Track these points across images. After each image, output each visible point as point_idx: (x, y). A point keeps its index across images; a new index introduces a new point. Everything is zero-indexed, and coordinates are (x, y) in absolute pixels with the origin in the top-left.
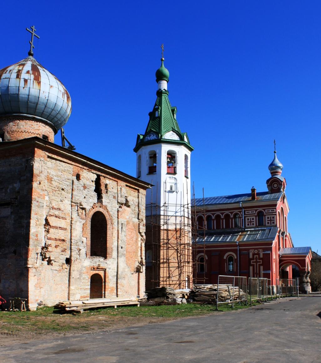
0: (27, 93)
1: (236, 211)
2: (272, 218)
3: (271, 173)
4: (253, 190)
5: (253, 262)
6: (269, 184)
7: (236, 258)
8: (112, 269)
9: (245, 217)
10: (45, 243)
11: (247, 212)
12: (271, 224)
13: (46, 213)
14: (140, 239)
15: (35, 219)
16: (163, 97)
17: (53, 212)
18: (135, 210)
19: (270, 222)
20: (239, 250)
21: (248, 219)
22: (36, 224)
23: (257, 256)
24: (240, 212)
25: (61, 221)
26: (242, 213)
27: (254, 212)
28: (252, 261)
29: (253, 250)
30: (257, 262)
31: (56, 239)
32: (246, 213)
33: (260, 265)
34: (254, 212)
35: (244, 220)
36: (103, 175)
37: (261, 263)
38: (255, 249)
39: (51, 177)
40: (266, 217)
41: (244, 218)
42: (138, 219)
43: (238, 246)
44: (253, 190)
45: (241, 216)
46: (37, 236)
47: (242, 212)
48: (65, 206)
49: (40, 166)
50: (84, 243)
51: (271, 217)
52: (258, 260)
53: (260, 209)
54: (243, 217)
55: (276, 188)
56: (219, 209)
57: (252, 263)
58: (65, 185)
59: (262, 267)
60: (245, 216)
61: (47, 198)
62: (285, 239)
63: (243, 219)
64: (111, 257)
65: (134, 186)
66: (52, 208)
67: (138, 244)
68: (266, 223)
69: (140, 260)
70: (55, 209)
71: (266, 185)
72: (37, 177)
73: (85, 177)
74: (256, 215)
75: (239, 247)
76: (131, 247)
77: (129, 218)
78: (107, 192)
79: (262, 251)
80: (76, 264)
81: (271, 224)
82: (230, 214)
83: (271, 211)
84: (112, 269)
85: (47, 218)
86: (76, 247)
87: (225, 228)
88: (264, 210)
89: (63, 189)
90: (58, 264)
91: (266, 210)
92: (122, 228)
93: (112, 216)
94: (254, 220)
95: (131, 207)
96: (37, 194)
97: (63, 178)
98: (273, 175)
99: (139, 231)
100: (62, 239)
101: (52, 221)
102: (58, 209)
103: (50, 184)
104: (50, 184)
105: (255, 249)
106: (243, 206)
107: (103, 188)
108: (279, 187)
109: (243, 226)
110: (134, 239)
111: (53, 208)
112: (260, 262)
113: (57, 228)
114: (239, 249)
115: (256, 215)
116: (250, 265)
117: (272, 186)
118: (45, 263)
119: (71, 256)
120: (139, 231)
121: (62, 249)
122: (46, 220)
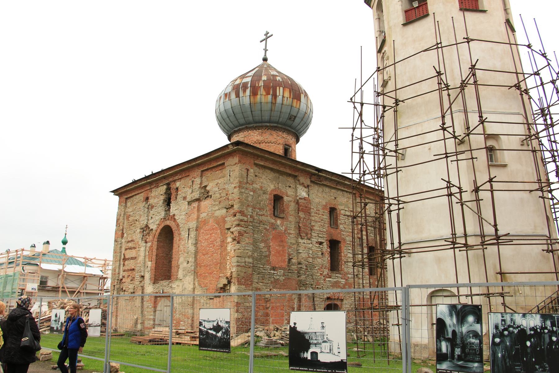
36: (171, 179)
64: (177, 279)
65: (215, 164)
67: (226, 249)
76: (210, 257)
86: (139, 274)
92: (189, 235)
111: (129, 242)
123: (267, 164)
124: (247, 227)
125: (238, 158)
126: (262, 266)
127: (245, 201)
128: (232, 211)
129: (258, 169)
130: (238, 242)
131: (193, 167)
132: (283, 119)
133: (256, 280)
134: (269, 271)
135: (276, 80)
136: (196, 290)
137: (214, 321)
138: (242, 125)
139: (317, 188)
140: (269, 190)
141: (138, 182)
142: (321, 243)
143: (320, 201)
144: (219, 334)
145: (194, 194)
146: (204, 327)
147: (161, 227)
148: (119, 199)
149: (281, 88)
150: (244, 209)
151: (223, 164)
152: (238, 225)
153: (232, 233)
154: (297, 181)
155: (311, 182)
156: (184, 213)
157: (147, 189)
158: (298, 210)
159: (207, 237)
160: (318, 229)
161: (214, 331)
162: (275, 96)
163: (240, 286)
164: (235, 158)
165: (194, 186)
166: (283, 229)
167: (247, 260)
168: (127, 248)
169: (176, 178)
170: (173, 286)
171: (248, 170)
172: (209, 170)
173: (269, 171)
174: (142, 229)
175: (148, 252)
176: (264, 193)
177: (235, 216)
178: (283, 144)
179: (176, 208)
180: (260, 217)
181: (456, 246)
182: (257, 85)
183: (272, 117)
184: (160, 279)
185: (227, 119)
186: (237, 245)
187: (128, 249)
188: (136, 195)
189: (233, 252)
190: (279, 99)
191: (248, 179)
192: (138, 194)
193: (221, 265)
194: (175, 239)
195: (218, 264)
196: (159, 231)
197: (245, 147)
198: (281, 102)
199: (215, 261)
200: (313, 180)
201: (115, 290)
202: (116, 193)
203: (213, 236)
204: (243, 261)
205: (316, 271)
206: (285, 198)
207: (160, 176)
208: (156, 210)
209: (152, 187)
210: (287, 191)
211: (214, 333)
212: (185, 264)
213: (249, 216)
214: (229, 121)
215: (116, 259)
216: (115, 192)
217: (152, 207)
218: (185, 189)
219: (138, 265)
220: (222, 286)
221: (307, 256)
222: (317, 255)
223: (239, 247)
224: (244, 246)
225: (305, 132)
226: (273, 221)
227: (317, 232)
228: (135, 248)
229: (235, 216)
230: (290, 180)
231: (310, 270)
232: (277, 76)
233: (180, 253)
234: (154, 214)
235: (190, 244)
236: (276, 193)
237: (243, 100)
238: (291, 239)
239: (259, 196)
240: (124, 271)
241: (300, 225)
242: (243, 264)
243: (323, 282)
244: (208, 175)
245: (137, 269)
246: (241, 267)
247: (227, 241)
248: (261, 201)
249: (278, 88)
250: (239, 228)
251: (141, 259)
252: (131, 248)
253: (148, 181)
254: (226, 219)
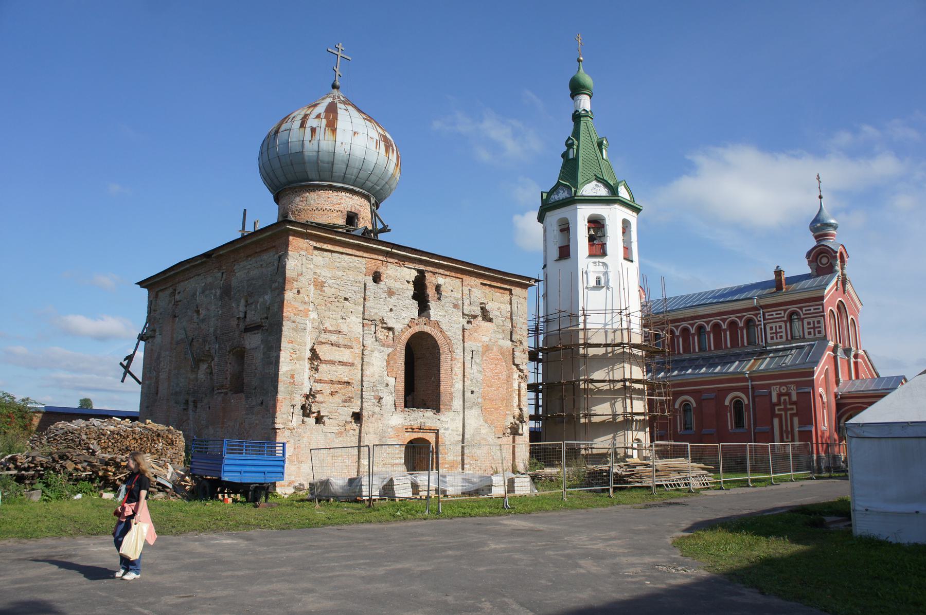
0: (316, 148)
1: (749, 315)
2: (816, 323)
3: (816, 238)
4: (778, 273)
5: (779, 410)
6: (811, 259)
7: (746, 402)
8: (452, 430)
9: (765, 325)
10: (311, 389)
11: (768, 315)
12: (815, 335)
13: (311, 339)
14: (516, 376)
15: (289, 349)
16: (582, 123)
17: (324, 337)
18: (503, 326)
19: (812, 330)
20: (752, 388)
21: (771, 328)
22: (290, 358)
23: (787, 398)
24: (756, 315)
25: (341, 351)
26: (760, 317)
27: (781, 314)
28: (777, 408)
29: (778, 387)
30: (786, 410)
31: (332, 382)
32: (767, 317)
33: (792, 415)
34: (781, 314)
35: (763, 330)
36: (431, 269)
37: (795, 411)
38: (781, 384)
39: (322, 281)
40: (805, 322)
41: (763, 328)
42: (511, 340)
43: (750, 381)
44: (778, 273)
45: (757, 323)
46: (292, 377)
47: (759, 316)
48: (351, 326)
49: (299, 265)
50: (389, 386)
51: (814, 322)
52: (789, 406)
53: (793, 308)
54: (761, 325)
55: (826, 264)
56: (716, 311)
57: (777, 412)
58: (350, 291)
59: (796, 420)
60: (765, 322)
61: (313, 315)
62: (856, 363)
63: (761, 328)
66: (323, 330)
67: (512, 385)
68: (806, 333)
69: (517, 412)
70: (330, 332)
71: (806, 261)
72: (293, 283)
73: (390, 276)
74: (785, 319)
75: (751, 382)
76: (495, 390)
77: (490, 340)
78: (439, 299)
79: (795, 388)
80: (371, 423)
81: (815, 335)
82: (738, 320)
83: (814, 309)
84: (452, 430)
85: (314, 348)
87: (714, 350)
88: (801, 308)
89: (346, 299)
90: (337, 422)
91: (804, 309)
92: (472, 358)
93: (451, 338)
94: (783, 329)
95: (494, 320)
96: (292, 309)
97: (346, 281)
98: (819, 241)
99: (513, 361)
100: (344, 381)
101: (324, 352)
102: (336, 331)
103: (321, 292)
104: (319, 293)
105: (781, 384)
106: (761, 304)
107: (431, 291)
108: (831, 263)
109: (762, 342)
110: (503, 376)
111: (326, 331)
112: (792, 409)
113: (333, 364)
114: (752, 385)
115: (785, 319)
116: (773, 415)
117: (817, 263)
118: (311, 420)
119: (361, 409)
120: (513, 361)
121: (344, 398)
122: (313, 350)
153: (521, 371)
159: (491, 367)
169: (441, 271)
187: (327, 343)
195: (504, 400)
199: (501, 396)
203: (498, 367)
215: (294, 356)
247: (514, 377)
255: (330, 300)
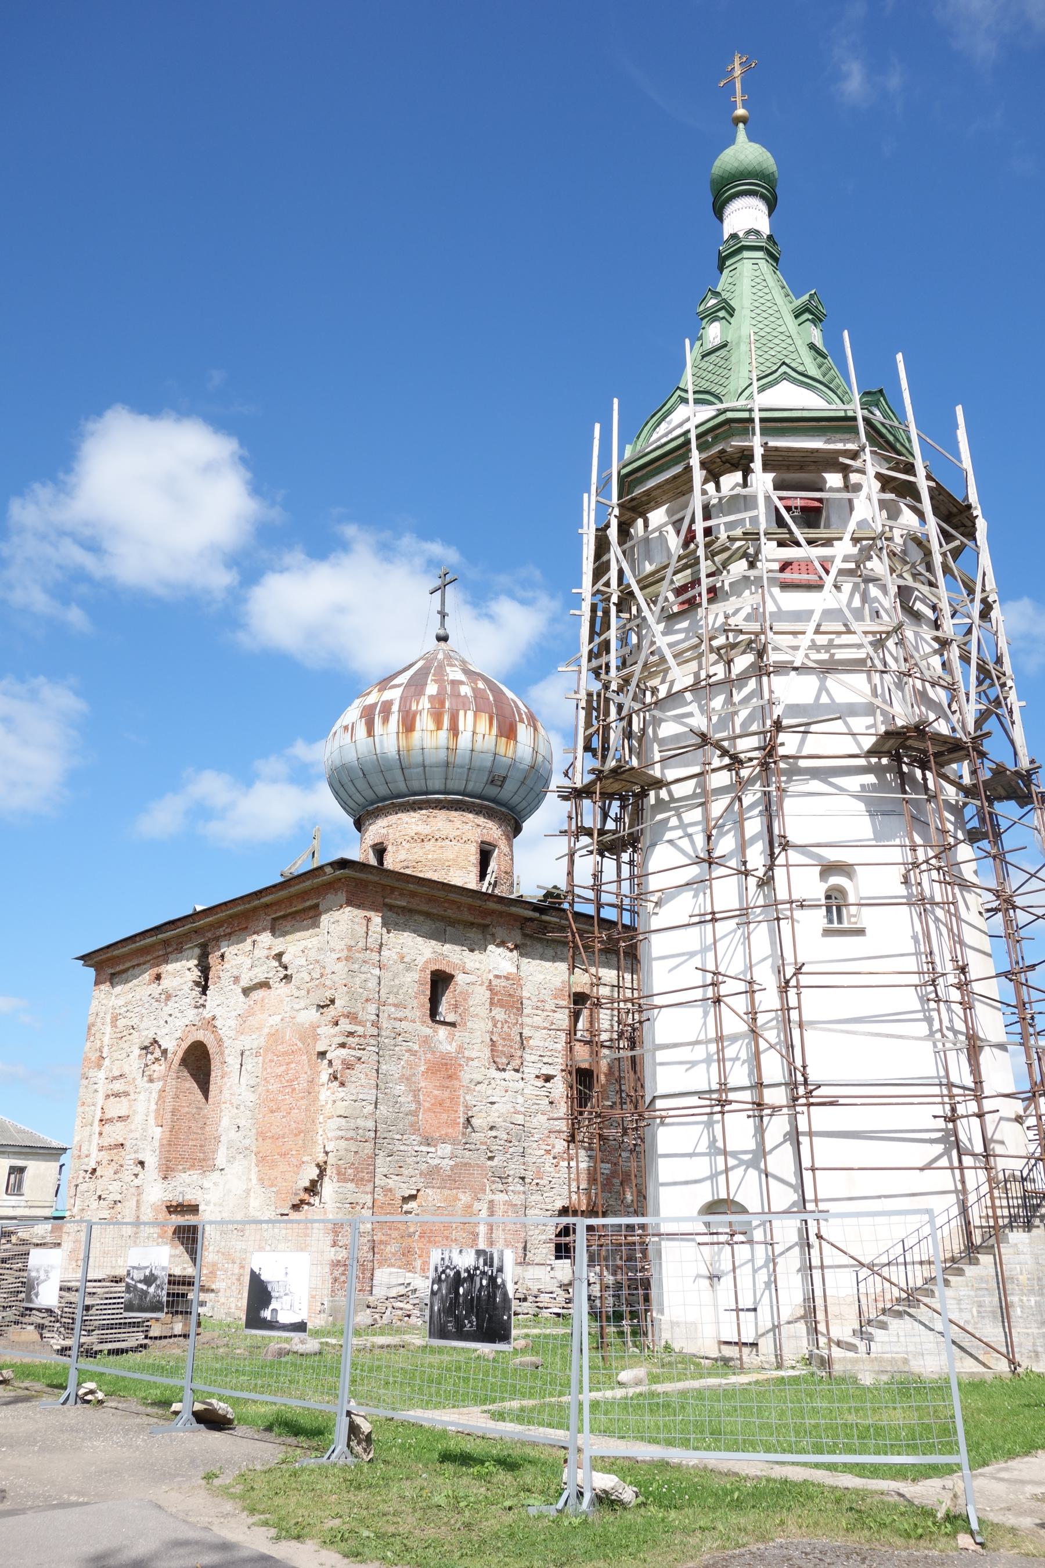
36: (209, 935)
67: (316, 1099)
76: (284, 1117)
84: (215, 1205)
123: (415, 904)
124: (364, 1049)
125: (344, 894)
126: (399, 1137)
127: (361, 990)
128: (331, 1012)
129: (394, 915)
130: (342, 1084)
131: (255, 909)
132: (476, 784)
133: (385, 1171)
134: (416, 1148)
135: (459, 695)
136: (252, 1194)
137: (146, 1268)
138: (384, 799)
139: (541, 950)
140: (421, 961)
141: (138, 939)
142: (548, 1078)
143: (549, 978)
144: (152, 1290)
145: (256, 970)
146: (132, 1279)
147: (185, 1045)
148: (97, 975)
149: (470, 714)
150: (358, 1008)
151: (317, 906)
152: (343, 1045)
154: (488, 937)
155: (525, 935)
156: (236, 1013)
157: (157, 954)
158: (492, 1004)
159: (279, 1071)
160: (541, 1044)
161: (146, 1284)
162: (454, 730)
163: (344, 1185)
164: (339, 893)
165: (256, 952)
166: (450, 1048)
167: (360, 1122)
168: (110, 1093)
169: (221, 931)
170: (206, 1185)
171: (369, 920)
172: (289, 918)
173: (422, 918)
174: (146, 1048)
175: (157, 1104)
176: (408, 969)
177: (336, 1024)
178: (476, 842)
179: (218, 1002)
180: (397, 1024)
181: (727, 1108)
182: (414, 708)
183: (448, 782)
184: (181, 1167)
185: (350, 784)
186: (340, 1089)
188: (133, 967)
189: (329, 1105)
190: (464, 741)
191: (369, 940)
192: (138, 965)
193: (305, 1132)
194: (213, 1074)
195: (300, 1133)
196: (180, 1054)
197: (361, 871)
198: (469, 746)
199: (294, 1125)
200: (528, 931)
201: (78, 1195)
202: (89, 963)
204: (353, 1126)
205: (535, 1145)
206: (460, 978)
207: (186, 927)
208: (176, 1005)
209: (169, 950)
210: (466, 960)
211: (145, 1287)
212: (233, 1134)
213: (369, 1024)
214: (355, 791)
216: (86, 958)
217: (169, 997)
218: (239, 958)
219: (132, 1135)
220: (307, 1184)
221: (512, 1110)
222: (537, 1107)
223: (342, 1094)
224: (354, 1092)
225: (536, 807)
226: (428, 1031)
227: (539, 1053)
228: (126, 1094)
229: (336, 1024)
230: (471, 935)
231: (517, 1144)
232: (462, 683)
233: (223, 1106)
234: (170, 1015)
235: (244, 1087)
236: (437, 967)
237: (381, 742)
238: (468, 1074)
239: (395, 976)
240: (101, 1149)
241: (494, 1039)
242: (351, 1134)
243: (552, 1169)
244: (286, 929)
245: (128, 1145)
246: (346, 1139)
248: (401, 986)
249: (461, 713)
250: (344, 1052)
251: (138, 1119)
252: (117, 1095)
253: (160, 936)
254: (319, 1031)
255: (119, 1035)
